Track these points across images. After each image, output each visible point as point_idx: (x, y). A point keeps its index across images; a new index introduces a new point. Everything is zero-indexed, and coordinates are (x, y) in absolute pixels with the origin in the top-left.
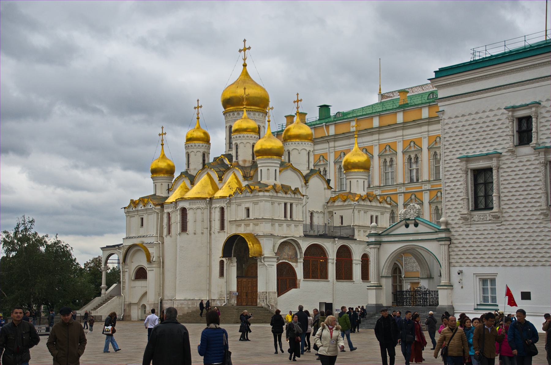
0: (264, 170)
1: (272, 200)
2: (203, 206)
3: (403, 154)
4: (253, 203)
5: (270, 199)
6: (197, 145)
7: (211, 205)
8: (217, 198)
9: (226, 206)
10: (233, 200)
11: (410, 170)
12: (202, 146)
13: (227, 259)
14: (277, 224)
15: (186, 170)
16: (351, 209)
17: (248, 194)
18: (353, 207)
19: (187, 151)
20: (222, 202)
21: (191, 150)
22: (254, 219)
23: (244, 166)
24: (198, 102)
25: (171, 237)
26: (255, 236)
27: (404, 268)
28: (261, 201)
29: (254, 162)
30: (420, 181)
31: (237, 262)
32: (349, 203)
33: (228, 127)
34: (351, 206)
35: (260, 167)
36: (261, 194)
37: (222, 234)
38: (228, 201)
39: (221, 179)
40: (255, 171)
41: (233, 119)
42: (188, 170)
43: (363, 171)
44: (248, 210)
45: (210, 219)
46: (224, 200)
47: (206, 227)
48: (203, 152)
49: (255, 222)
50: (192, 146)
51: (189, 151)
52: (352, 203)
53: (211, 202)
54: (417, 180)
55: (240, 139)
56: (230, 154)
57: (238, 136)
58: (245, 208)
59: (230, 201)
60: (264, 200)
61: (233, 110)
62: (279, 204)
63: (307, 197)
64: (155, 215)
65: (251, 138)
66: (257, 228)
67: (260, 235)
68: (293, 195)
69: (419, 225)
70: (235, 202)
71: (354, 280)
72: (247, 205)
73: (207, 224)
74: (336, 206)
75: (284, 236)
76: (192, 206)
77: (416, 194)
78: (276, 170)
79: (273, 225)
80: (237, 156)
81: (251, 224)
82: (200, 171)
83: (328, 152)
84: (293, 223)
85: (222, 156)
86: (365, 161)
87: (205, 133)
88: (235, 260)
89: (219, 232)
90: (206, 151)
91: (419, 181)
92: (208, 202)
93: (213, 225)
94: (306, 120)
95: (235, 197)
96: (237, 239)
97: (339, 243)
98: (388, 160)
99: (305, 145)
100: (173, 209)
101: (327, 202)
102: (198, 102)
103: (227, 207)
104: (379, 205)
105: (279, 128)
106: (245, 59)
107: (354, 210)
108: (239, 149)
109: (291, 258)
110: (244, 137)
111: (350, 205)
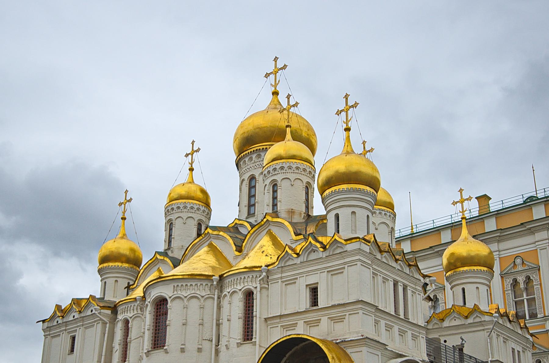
0: (344, 214)
1: (374, 266)
2: (203, 294)
3: (501, 277)
4: (328, 271)
5: (370, 263)
6: (189, 206)
7: (221, 291)
8: (237, 271)
9: (258, 286)
10: (276, 274)
11: (516, 303)
12: (198, 209)
14: (383, 323)
15: (166, 250)
16: (484, 330)
17: (313, 256)
18: (491, 327)
19: (168, 218)
20: (249, 280)
21: (177, 215)
22: (334, 306)
23: (290, 221)
24: (193, 145)
26: (337, 343)
28: (352, 264)
29: (309, 216)
30: (539, 316)
32: (478, 320)
33: (246, 180)
34: (483, 325)
36: (350, 247)
37: (247, 347)
38: (264, 274)
39: (239, 249)
40: (317, 226)
41: (256, 164)
42: (169, 249)
43: (486, 271)
44: (314, 291)
45: (217, 320)
46: (254, 275)
47: (207, 336)
48: (200, 220)
49: (334, 313)
50: (178, 208)
51: (173, 217)
52: (487, 318)
53: (221, 287)
54: (533, 316)
55: (282, 172)
56: (251, 222)
57: (278, 167)
58: (307, 286)
59: (268, 277)
60: (360, 260)
61: (258, 148)
62: (385, 280)
63: (431, 278)
65: (303, 173)
66: (338, 326)
67: (351, 340)
68: (408, 269)
70: (281, 278)
72: (311, 280)
73: (210, 331)
74: (445, 327)
75: (397, 352)
76: (179, 292)
78: (368, 216)
79: (377, 322)
80: (274, 205)
81: (325, 321)
84: (410, 329)
86: (485, 256)
87: (203, 192)
89: (239, 345)
90: (204, 219)
92: (215, 283)
93: (224, 331)
95: (279, 266)
96: (287, 355)
99: (385, 217)
101: (427, 321)
102: (193, 145)
103: (261, 289)
104: (520, 332)
106: (275, 86)
107: (491, 331)
108: (279, 191)
110: (290, 168)
111: (481, 323)
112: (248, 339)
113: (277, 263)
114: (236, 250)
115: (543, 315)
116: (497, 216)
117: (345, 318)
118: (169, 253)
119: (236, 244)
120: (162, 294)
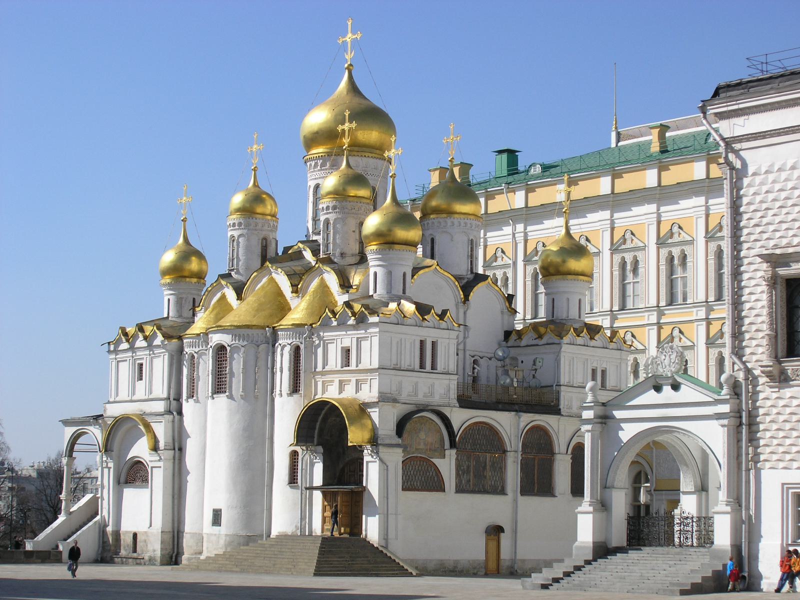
13: (304, 448)
25: (197, 401)
27: (654, 471)
31: (324, 454)
35: (375, 266)
37: (296, 396)
39: (295, 290)
42: (233, 270)
49: (361, 377)
54: (685, 299)
58: (342, 348)
64: (166, 357)
69: (682, 386)
71: (557, 494)
72: (347, 343)
77: (681, 326)
82: (255, 274)
83: (511, 240)
85: (301, 245)
88: (320, 449)
91: (686, 301)
94: (471, 178)
97: (527, 419)
98: (629, 258)
100: (201, 347)
105: (418, 192)
109: (430, 449)
112: (296, 391)
113: (319, 323)
114: (292, 292)
115: (692, 300)
116: (660, 165)
117: (367, 381)
118: (233, 273)
119: (293, 284)
120: (222, 342)
